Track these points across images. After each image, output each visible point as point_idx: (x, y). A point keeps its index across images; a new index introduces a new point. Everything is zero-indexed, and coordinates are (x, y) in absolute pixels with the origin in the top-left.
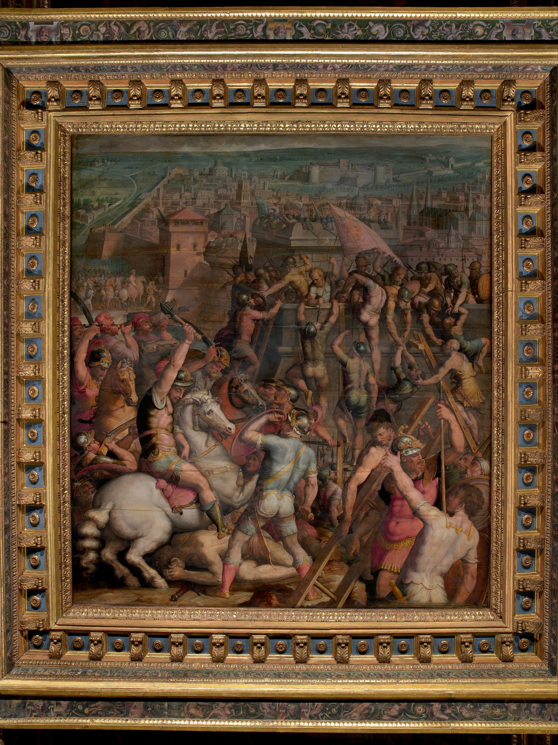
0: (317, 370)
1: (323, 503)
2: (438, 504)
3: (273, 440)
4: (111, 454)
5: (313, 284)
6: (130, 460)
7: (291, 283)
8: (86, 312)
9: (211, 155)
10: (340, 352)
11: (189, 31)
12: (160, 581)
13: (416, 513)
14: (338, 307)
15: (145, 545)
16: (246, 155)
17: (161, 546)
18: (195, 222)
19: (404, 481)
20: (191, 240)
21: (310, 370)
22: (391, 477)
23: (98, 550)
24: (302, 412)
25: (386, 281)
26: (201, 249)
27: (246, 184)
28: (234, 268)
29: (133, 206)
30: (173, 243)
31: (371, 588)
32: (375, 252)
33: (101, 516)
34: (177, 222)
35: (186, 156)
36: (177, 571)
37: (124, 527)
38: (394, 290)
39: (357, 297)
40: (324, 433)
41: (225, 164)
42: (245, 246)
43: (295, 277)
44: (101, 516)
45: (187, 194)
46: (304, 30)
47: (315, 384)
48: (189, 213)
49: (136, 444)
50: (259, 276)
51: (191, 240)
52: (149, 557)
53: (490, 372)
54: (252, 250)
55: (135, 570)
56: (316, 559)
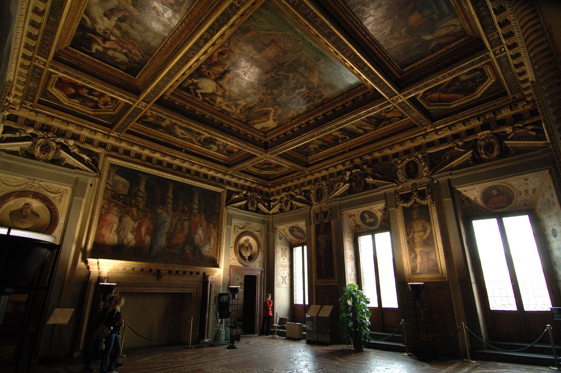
0: (275, 92)
1: (251, 108)
2: (274, 120)
3: (252, 95)
4: (208, 73)
5: (293, 79)
6: (213, 77)
7: (289, 76)
8: (229, 44)
9: (302, 37)
10: (284, 92)
11: (329, 32)
12: (201, 98)
13: (268, 119)
14: (293, 86)
15: (202, 91)
16: (311, 45)
17: (207, 93)
18: (280, 48)
19: (272, 114)
20: (275, 51)
21: (274, 91)
22: (270, 112)
23: (189, 85)
24: (263, 94)
25: (308, 88)
26: (275, 54)
27: (303, 51)
28: (279, 64)
29: (267, 30)
30: (270, 47)
31: (247, 121)
32: (314, 83)
33: (195, 81)
34: (276, 44)
35: (296, 32)
36: (207, 99)
37: (200, 85)
38: (308, 91)
39: (299, 87)
40: (264, 100)
41: (304, 42)
42: (286, 62)
43: (291, 75)
44: (195, 81)
45: (286, 41)
46: (353, 56)
47: (272, 94)
48: (282, 45)
49: (218, 76)
50: (283, 69)
51: (275, 51)
52: (201, 93)
53: (308, 112)
54: (287, 64)
55: (196, 94)
56: (241, 113)
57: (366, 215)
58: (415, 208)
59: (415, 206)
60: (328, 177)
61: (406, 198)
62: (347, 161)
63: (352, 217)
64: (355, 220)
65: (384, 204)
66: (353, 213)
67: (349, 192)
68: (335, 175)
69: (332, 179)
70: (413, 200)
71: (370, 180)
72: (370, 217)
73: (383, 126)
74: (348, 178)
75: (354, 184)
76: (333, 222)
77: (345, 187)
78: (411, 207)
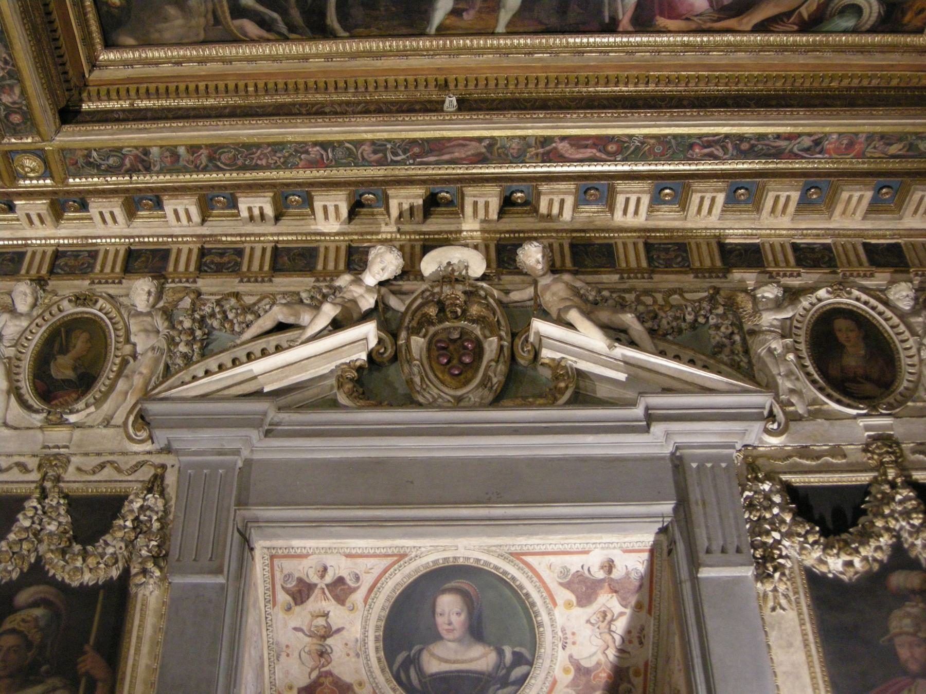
57: (449, 609)
58: (902, 597)
59: (898, 580)
60: (183, 263)
61: (834, 514)
62: (409, 182)
63: (316, 603)
64: (328, 632)
65: (647, 538)
66: (340, 567)
67: (369, 382)
68: (257, 262)
69: (209, 285)
70: (885, 540)
71: (576, 342)
72: (476, 631)
73: (762, 27)
74: (368, 302)
75: (418, 343)
76: (150, 594)
77: (327, 350)
78: (874, 581)
